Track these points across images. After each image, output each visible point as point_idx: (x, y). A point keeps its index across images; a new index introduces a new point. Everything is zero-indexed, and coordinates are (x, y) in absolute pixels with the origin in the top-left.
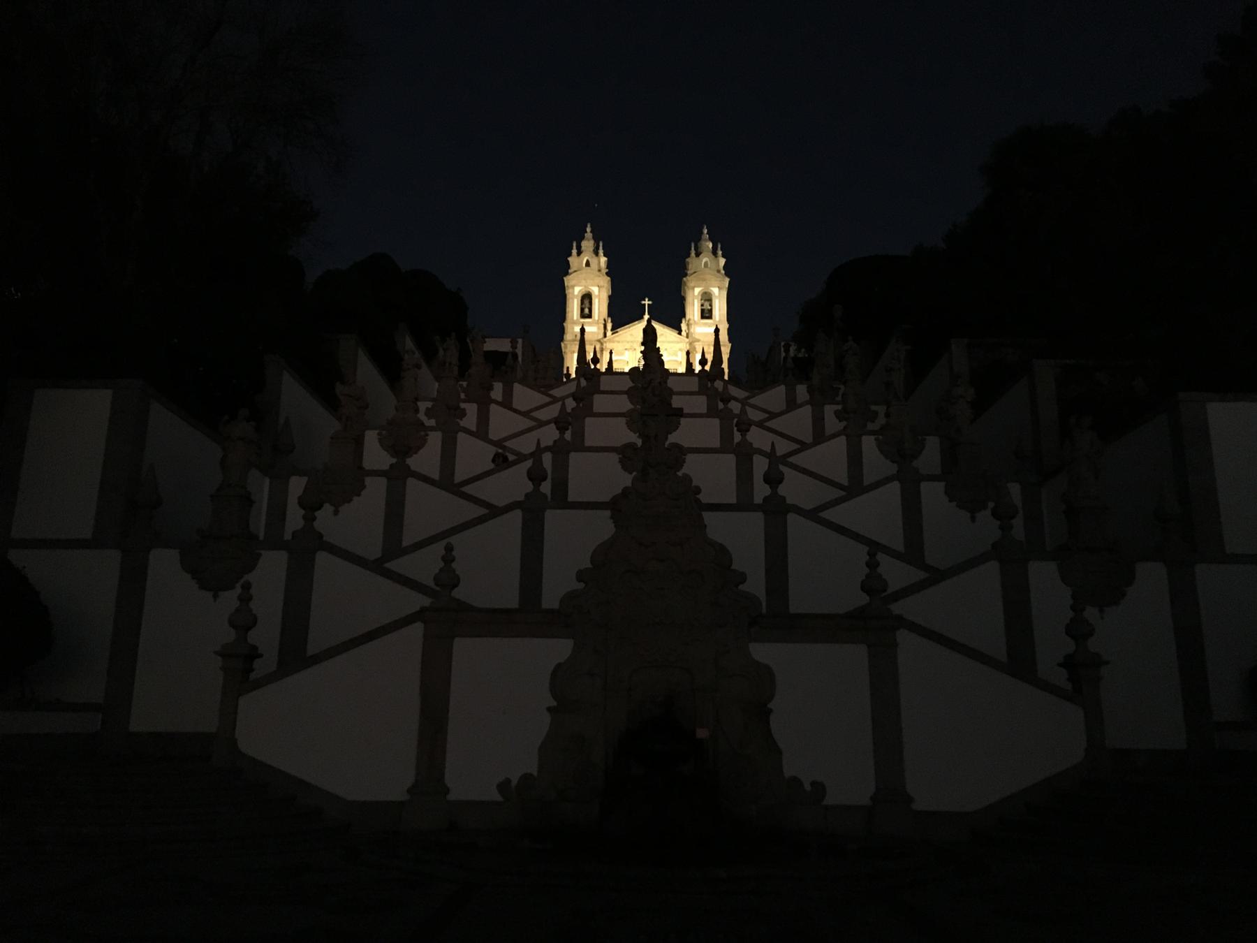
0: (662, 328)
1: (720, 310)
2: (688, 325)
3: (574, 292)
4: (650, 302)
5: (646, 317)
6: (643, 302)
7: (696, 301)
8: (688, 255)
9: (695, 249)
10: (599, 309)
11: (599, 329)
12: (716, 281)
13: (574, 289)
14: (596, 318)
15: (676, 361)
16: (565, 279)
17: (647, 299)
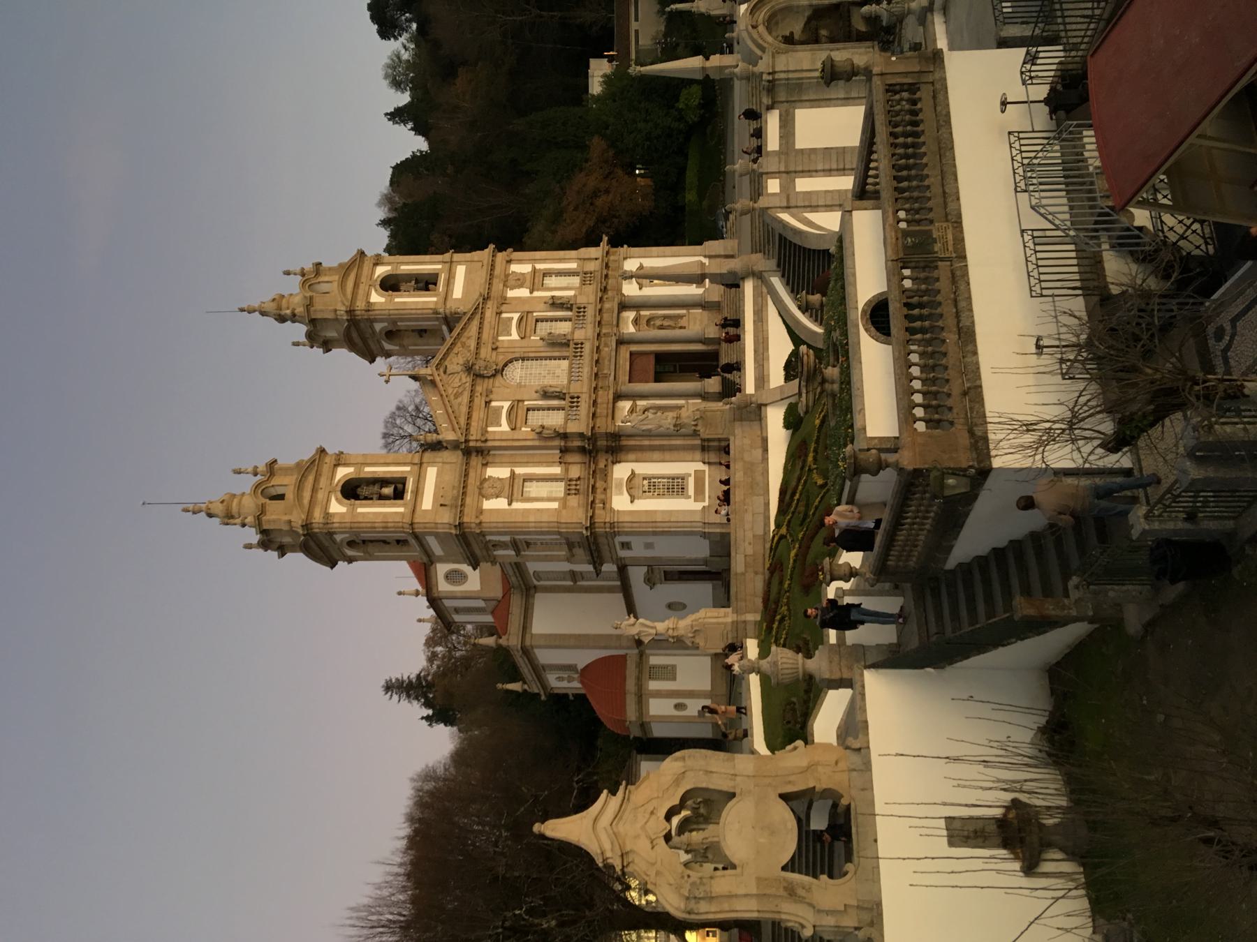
3: (342, 515)
11: (432, 463)
13: (334, 514)
14: (408, 469)
15: (520, 319)
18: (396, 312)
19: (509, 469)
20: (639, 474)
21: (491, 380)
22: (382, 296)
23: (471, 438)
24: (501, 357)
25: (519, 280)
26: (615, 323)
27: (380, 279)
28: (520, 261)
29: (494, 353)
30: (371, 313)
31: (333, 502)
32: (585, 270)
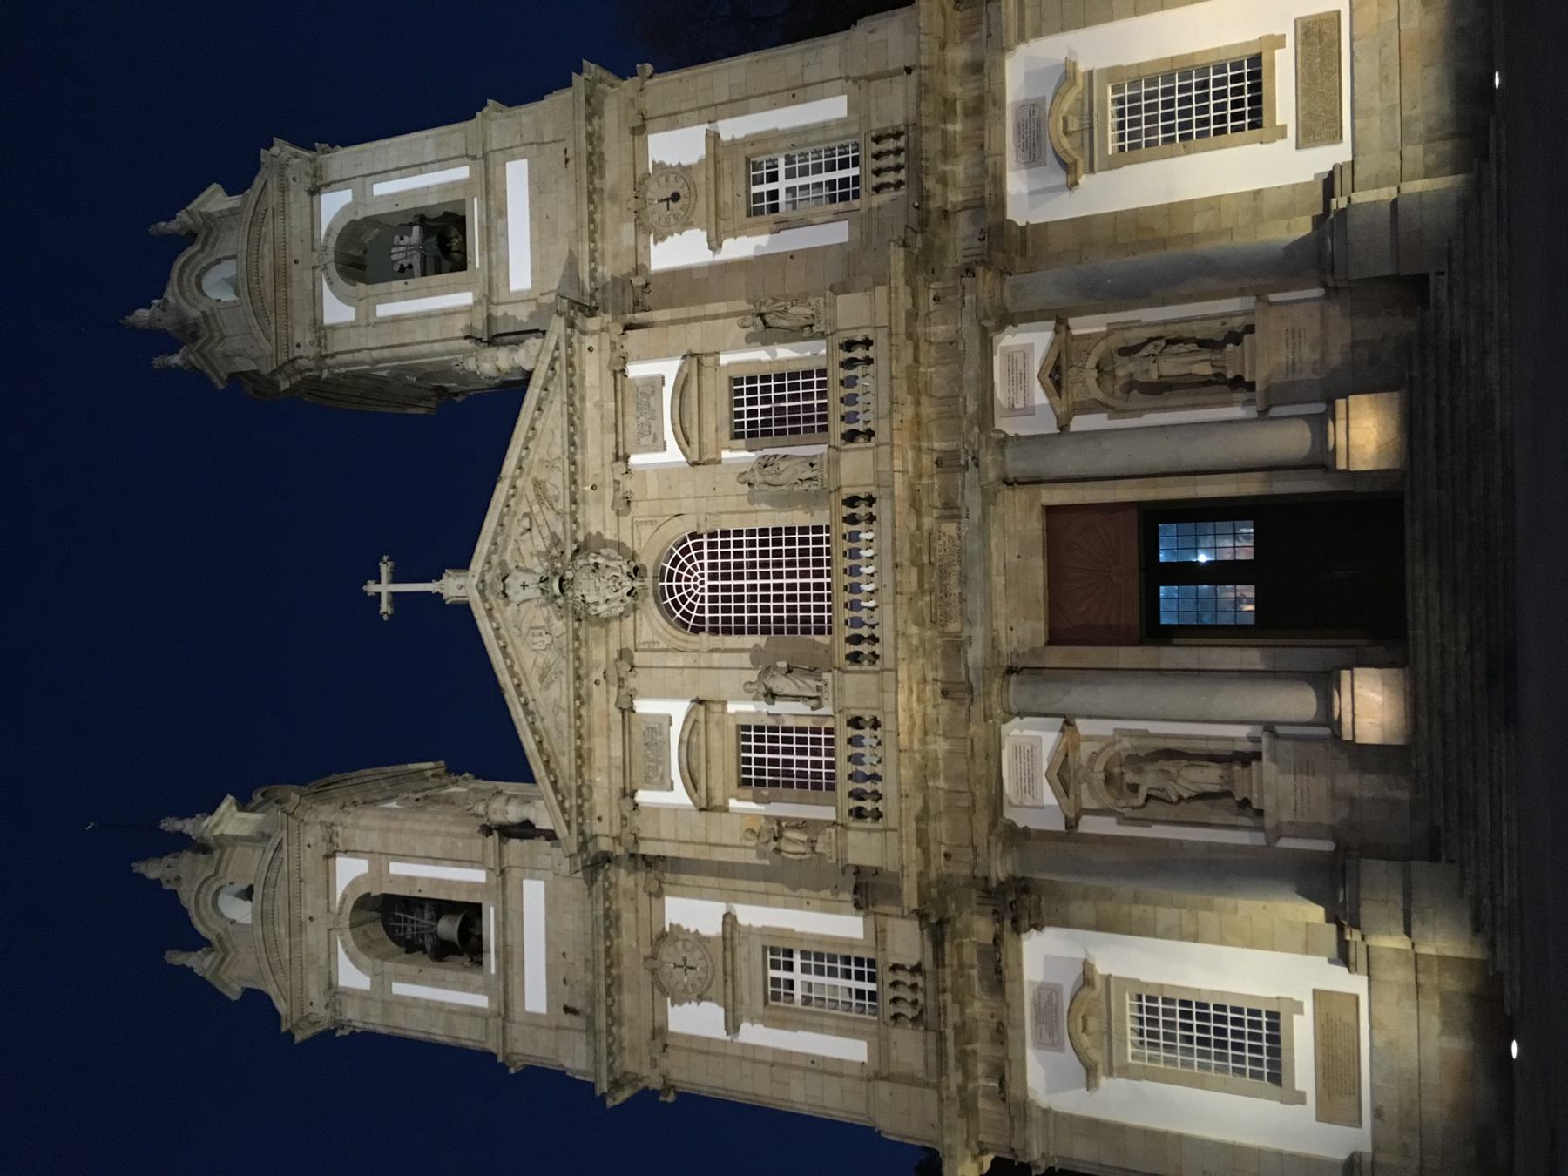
0: (501, 492)
1: (419, 167)
2: (494, 340)
3: (363, 996)
4: (385, 569)
5: (451, 586)
6: (385, 607)
7: (384, 310)
8: (195, 378)
9: (173, 351)
10: (436, 861)
11: (532, 871)
12: (283, 210)
13: (349, 993)
14: (478, 876)
16: (299, 1037)
17: (372, 588)
18: (386, 353)
19: (720, 908)
20: (1108, 978)
21: (629, 622)
22: (344, 298)
23: (598, 828)
24: (647, 531)
25: (676, 197)
26: (972, 408)
27: (332, 243)
28: (673, 120)
29: (626, 521)
30: (329, 361)
31: (342, 957)
32: (877, 126)
